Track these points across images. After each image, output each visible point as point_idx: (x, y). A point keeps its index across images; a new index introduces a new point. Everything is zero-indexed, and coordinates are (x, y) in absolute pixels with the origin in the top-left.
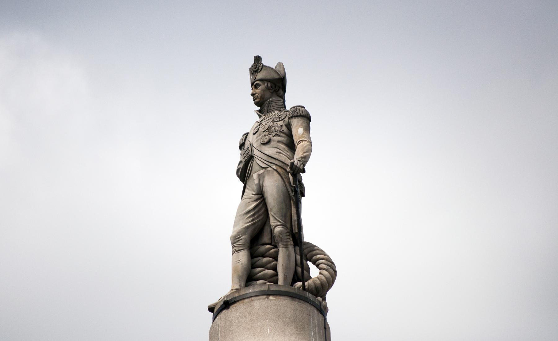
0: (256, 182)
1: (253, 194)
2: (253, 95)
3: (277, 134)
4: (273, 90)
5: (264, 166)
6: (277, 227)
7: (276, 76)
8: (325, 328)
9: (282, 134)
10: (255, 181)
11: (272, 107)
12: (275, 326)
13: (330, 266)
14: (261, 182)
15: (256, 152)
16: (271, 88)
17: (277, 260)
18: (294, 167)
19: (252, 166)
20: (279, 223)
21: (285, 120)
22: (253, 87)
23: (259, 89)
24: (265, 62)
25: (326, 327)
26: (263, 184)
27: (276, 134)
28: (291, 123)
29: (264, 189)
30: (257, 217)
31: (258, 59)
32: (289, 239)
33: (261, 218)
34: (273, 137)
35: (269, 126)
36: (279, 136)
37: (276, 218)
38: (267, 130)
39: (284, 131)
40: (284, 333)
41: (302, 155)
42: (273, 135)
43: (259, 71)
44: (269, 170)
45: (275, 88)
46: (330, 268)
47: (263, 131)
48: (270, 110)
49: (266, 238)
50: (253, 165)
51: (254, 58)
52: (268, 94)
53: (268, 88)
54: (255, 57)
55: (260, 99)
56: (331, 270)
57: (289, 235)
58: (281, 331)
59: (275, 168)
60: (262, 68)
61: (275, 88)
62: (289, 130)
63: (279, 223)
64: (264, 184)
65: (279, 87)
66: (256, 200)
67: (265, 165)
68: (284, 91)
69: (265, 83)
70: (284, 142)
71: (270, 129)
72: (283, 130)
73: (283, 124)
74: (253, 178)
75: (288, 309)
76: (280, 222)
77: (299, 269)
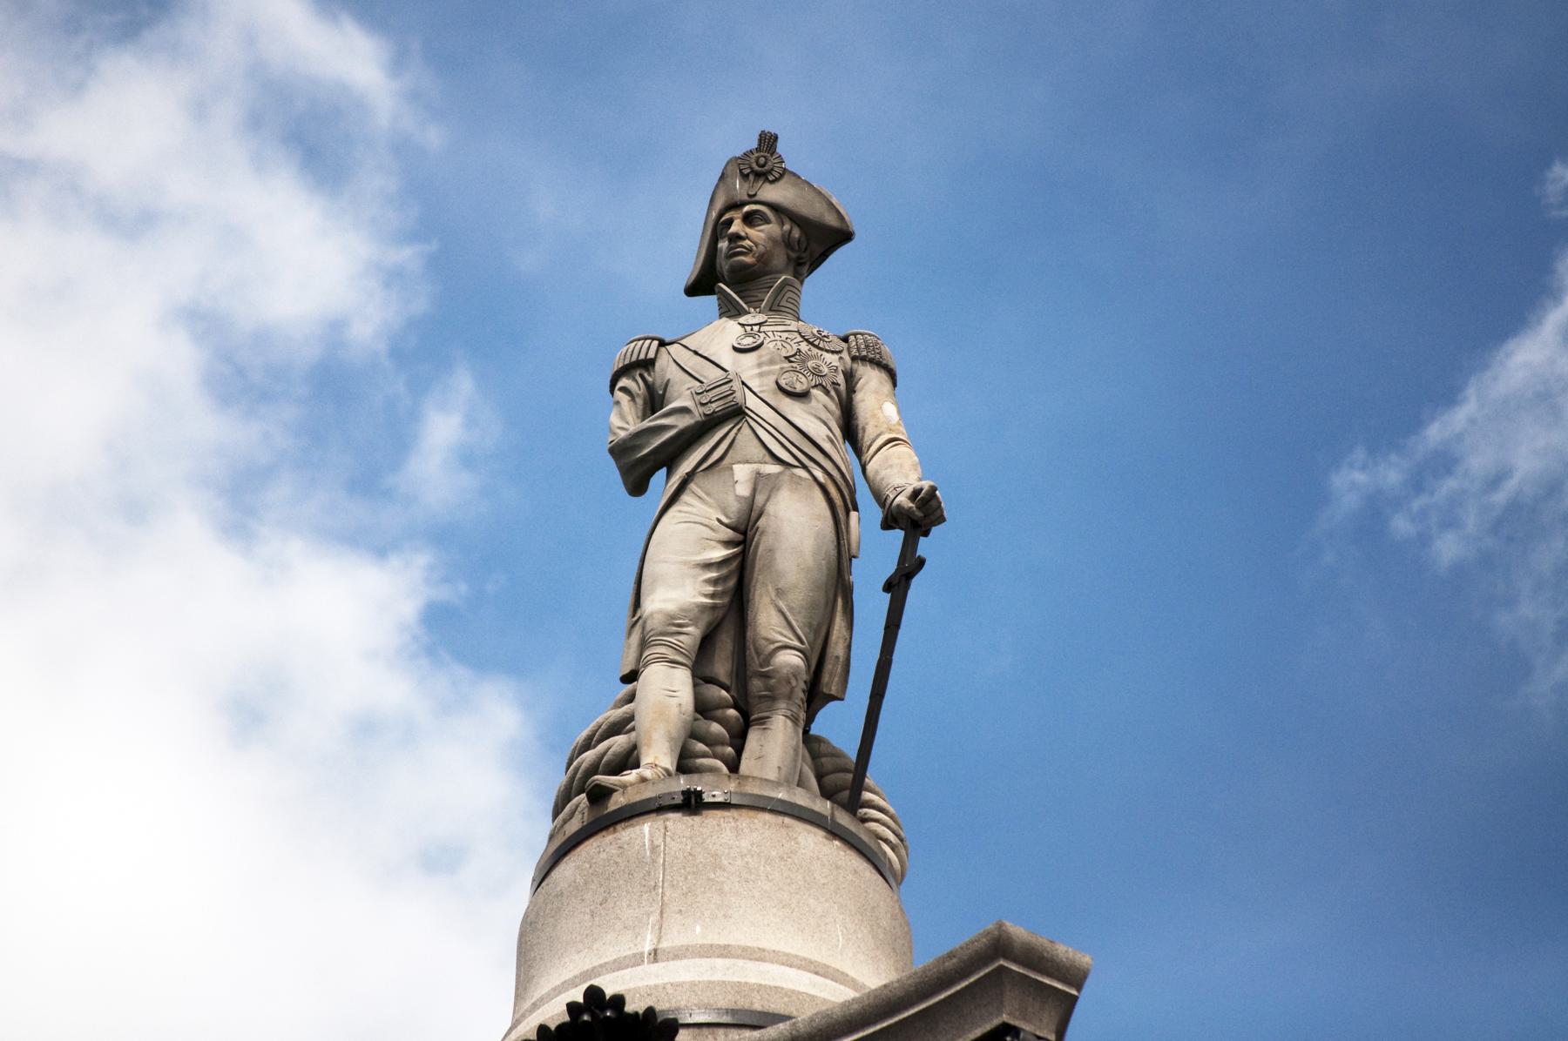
0: (743, 490)
1: (719, 520)
3: (824, 384)
6: (789, 651)
7: (831, 220)
10: (737, 486)
14: (760, 499)
18: (933, 503)
20: (796, 643)
26: (764, 505)
31: (768, 142)
37: (794, 623)
38: (792, 359)
43: (771, 178)
44: (800, 477)
45: (805, 251)
50: (739, 437)
52: (779, 259)
53: (787, 241)
55: (757, 261)
60: (782, 176)
63: (796, 643)
64: (770, 508)
67: (788, 454)
69: (783, 224)
74: (733, 475)
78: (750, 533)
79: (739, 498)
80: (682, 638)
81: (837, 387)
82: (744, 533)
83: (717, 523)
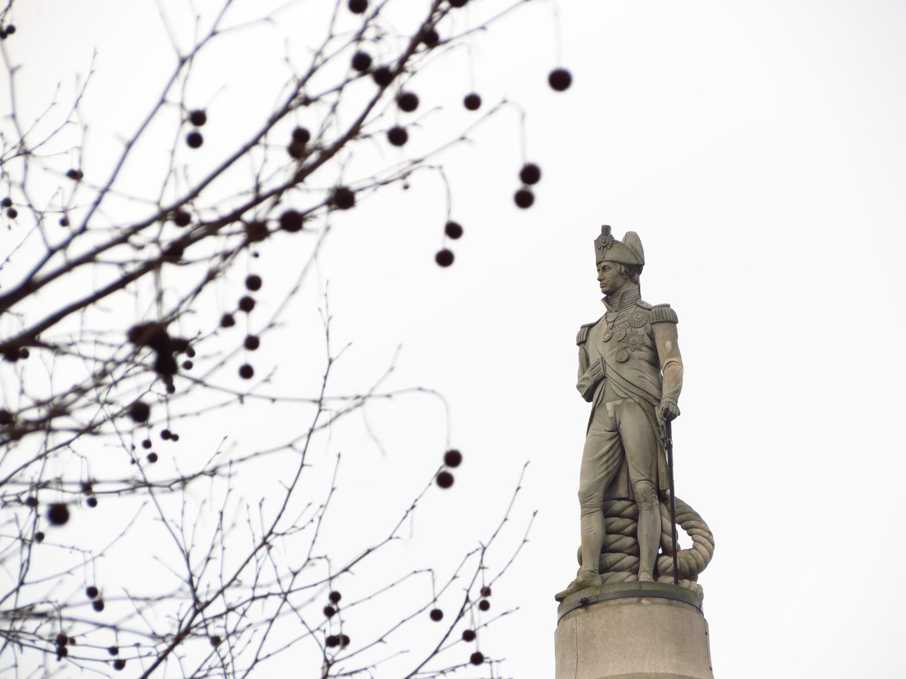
0: (611, 414)
1: (605, 430)
2: (600, 280)
3: (638, 347)
6: (640, 482)
13: (707, 538)
14: (618, 416)
16: (625, 274)
18: (668, 414)
20: (643, 478)
21: (646, 326)
23: (609, 274)
26: (620, 419)
28: (655, 332)
29: (621, 426)
30: (613, 463)
31: (606, 230)
33: (615, 464)
34: (633, 351)
35: (626, 334)
37: (639, 470)
42: (633, 350)
43: (609, 247)
44: (630, 403)
45: (630, 272)
46: (707, 541)
47: (618, 340)
49: (622, 491)
50: (606, 389)
52: (620, 281)
53: (621, 274)
54: (603, 226)
59: (637, 401)
61: (630, 272)
68: (640, 274)
75: (666, 619)
78: (619, 430)
79: (610, 418)
83: (606, 432)
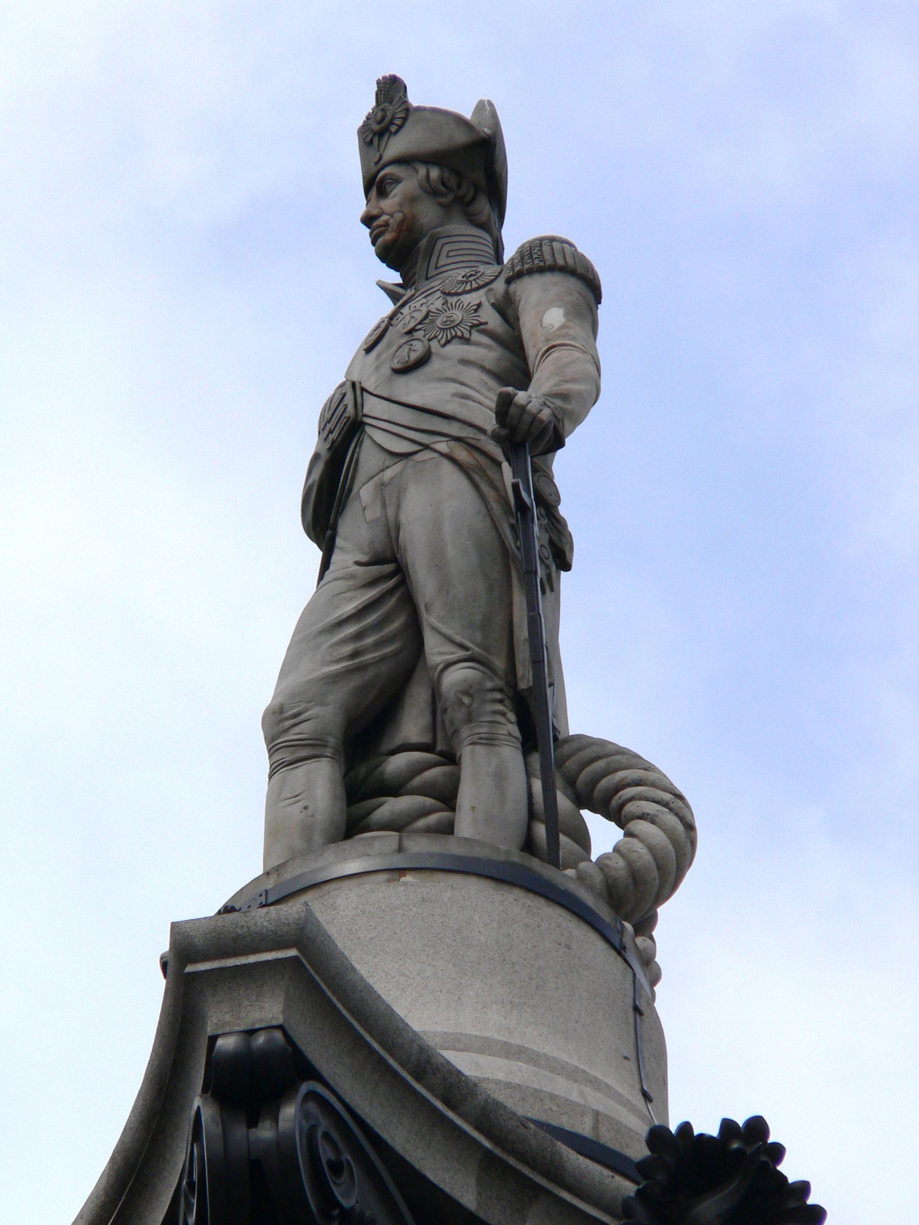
0: (374, 512)
1: (358, 563)
2: (368, 220)
3: (459, 334)
4: (450, 197)
5: (402, 447)
6: (452, 668)
7: (461, 137)
8: (637, 1010)
9: (476, 336)
11: (448, 256)
12: (418, 974)
13: (666, 805)
15: (373, 406)
16: (443, 189)
17: (453, 808)
18: (513, 410)
19: (357, 460)
20: (461, 654)
21: (494, 286)
22: (374, 192)
24: (415, 98)
25: (642, 1006)
27: (456, 336)
28: (518, 298)
30: (377, 645)
32: (503, 714)
34: (444, 346)
36: (467, 341)
39: (486, 323)
40: (456, 998)
41: (556, 388)
42: (443, 341)
43: (393, 128)
45: (459, 186)
48: (436, 268)
51: (375, 88)
52: (428, 213)
53: (431, 191)
54: (378, 82)
56: (671, 819)
57: (501, 701)
58: (444, 991)
60: (405, 119)
61: (459, 186)
62: (513, 329)
63: (461, 654)
64: (403, 518)
65: (477, 188)
66: (373, 583)
67: (406, 443)
69: (417, 171)
70: (487, 364)
71: (433, 321)
72: (483, 320)
73: (484, 300)
75: (476, 918)
76: (466, 648)
77: (541, 830)
80: (297, 729)
81: (482, 327)
82: (394, 559)
